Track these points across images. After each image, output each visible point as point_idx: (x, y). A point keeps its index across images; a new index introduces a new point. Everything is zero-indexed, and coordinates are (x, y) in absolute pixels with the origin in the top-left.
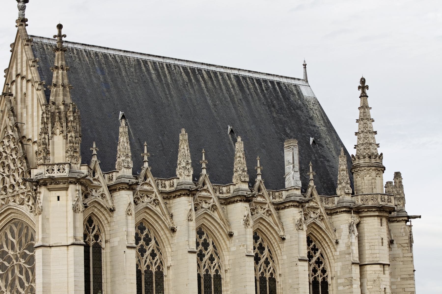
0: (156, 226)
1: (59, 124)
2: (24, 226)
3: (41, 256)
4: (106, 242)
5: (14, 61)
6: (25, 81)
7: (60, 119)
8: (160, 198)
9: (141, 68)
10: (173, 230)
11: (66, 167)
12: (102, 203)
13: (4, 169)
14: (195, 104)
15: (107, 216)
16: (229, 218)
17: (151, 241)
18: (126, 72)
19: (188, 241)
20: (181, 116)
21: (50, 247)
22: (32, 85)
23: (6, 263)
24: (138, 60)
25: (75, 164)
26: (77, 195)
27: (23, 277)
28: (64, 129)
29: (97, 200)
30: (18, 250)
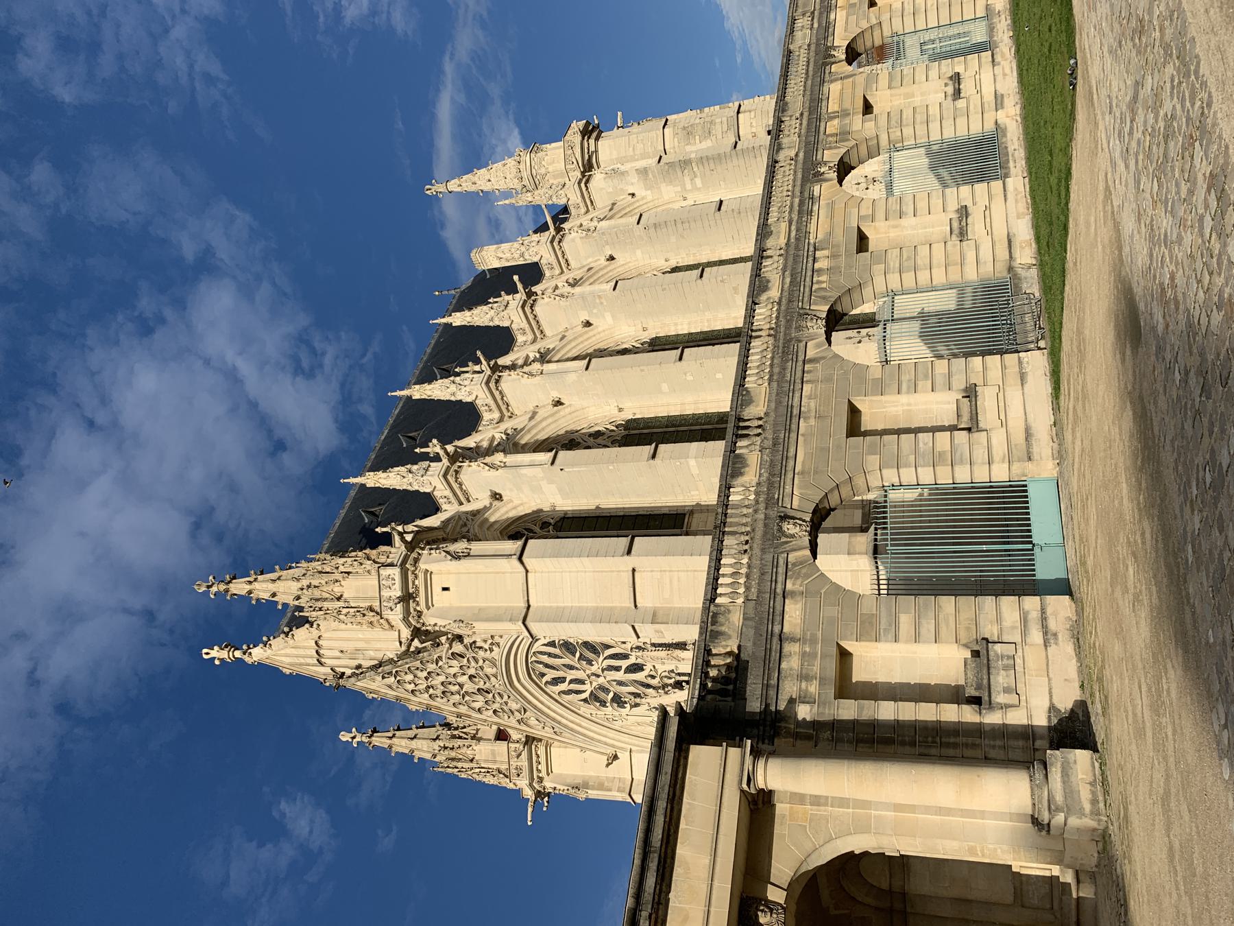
11: (385, 572)
21: (529, 606)
27: (624, 664)
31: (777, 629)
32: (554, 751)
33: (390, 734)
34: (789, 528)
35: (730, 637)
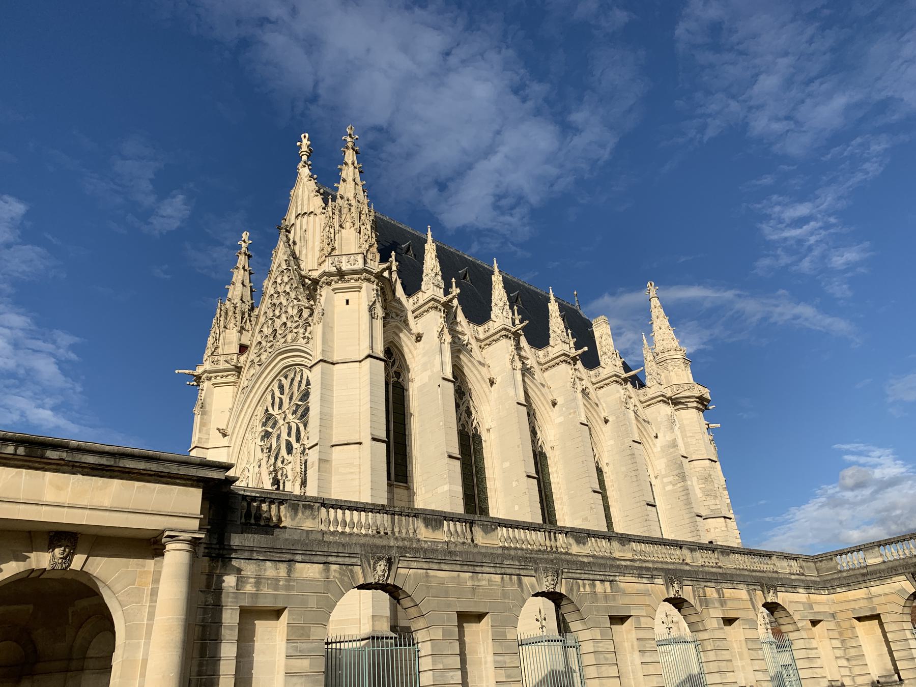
11: (360, 258)
21: (334, 364)
31: (299, 558)
32: (230, 389)
33: (246, 267)
34: (381, 566)
35: (293, 519)
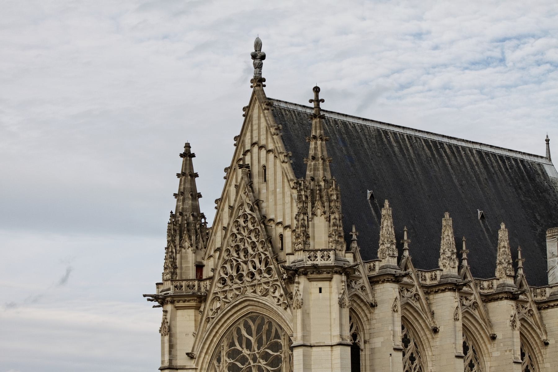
0: (416, 325)
1: (320, 203)
2: (266, 321)
3: (301, 357)
4: (365, 342)
5: (247, 128)
6: (263, 152)
7: (321, 197)
8: (421, 293)
9: (382, 139)
10: (435, 331)
11: (331, 254)
12: (362, 297)
13: (238, 254)
14: (442, 183)
15: (367, 312)
16: (491, 318)
17: (409, 342)
18: (368, 144)
19: (455, 343)
20: (429, 196)
21: (311, 346)
22: (275, 156)
23: (239, 364)
24: (378, 130)
25: (340, 250)
26: (343, 287)
28: (327, 209)
29: (357, 293)
30: (256, 349)
32: (191, 313)
